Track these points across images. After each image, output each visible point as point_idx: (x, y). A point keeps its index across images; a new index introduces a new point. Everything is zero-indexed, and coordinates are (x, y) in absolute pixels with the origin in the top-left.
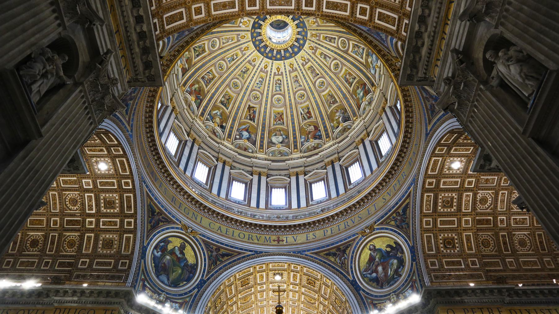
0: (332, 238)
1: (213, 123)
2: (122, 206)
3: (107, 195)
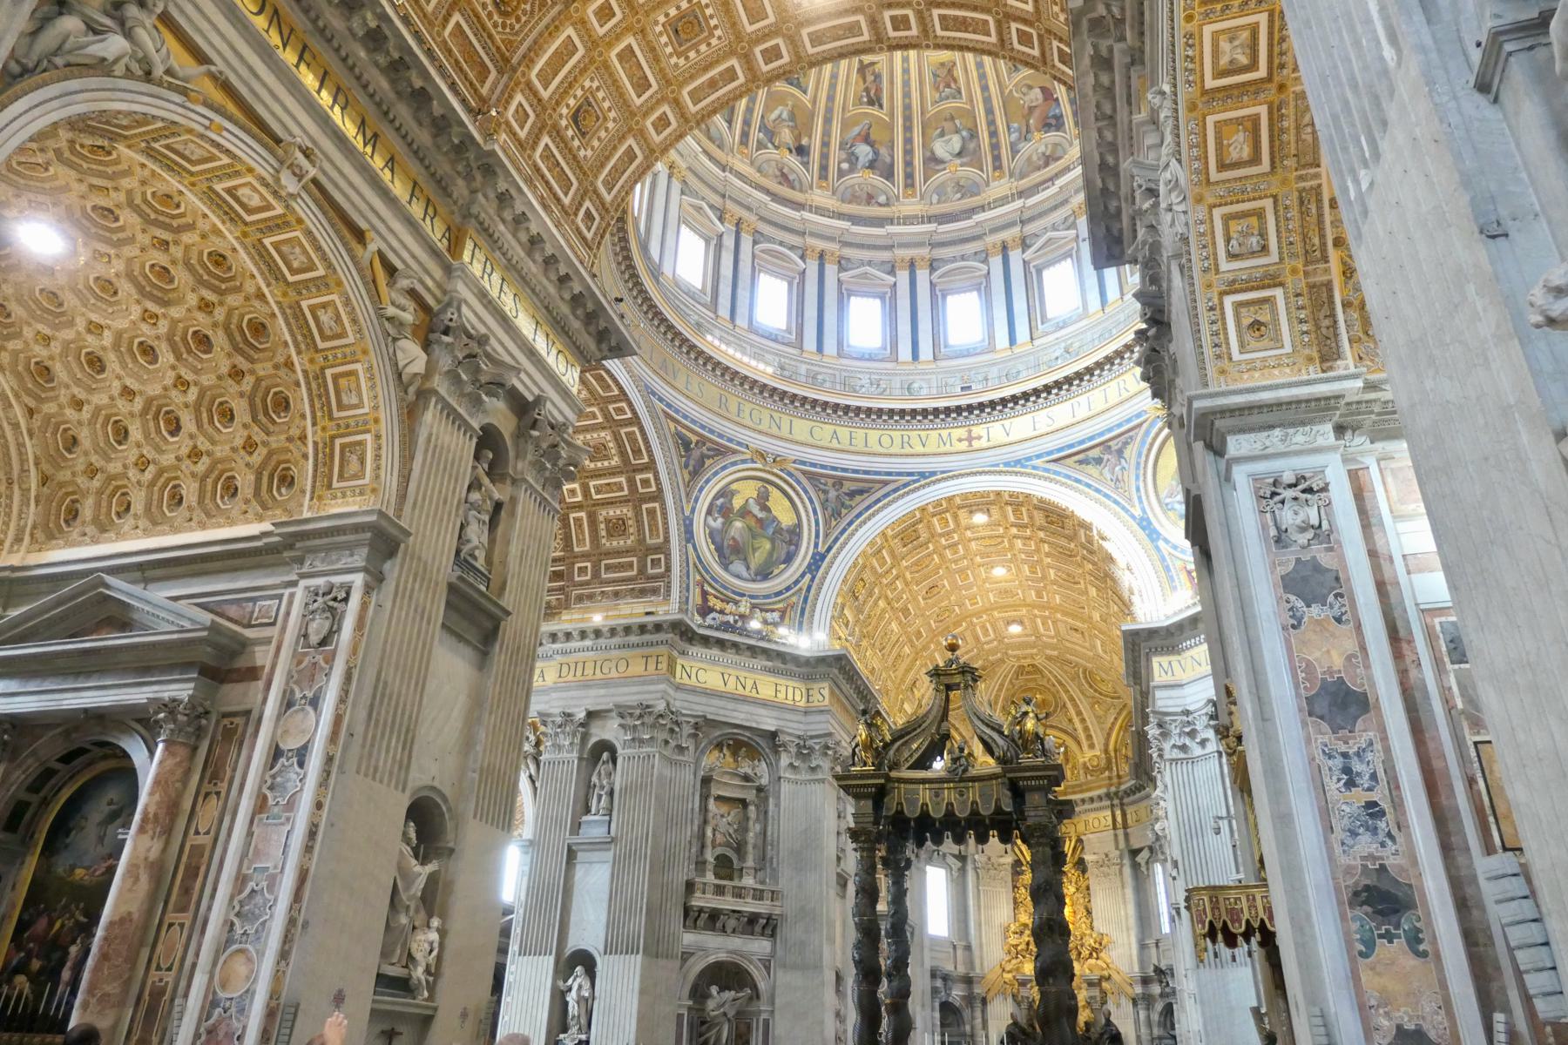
0: (1089, 423)
1: (777, 148)
2: (622, 453)
3: (588, 437)
